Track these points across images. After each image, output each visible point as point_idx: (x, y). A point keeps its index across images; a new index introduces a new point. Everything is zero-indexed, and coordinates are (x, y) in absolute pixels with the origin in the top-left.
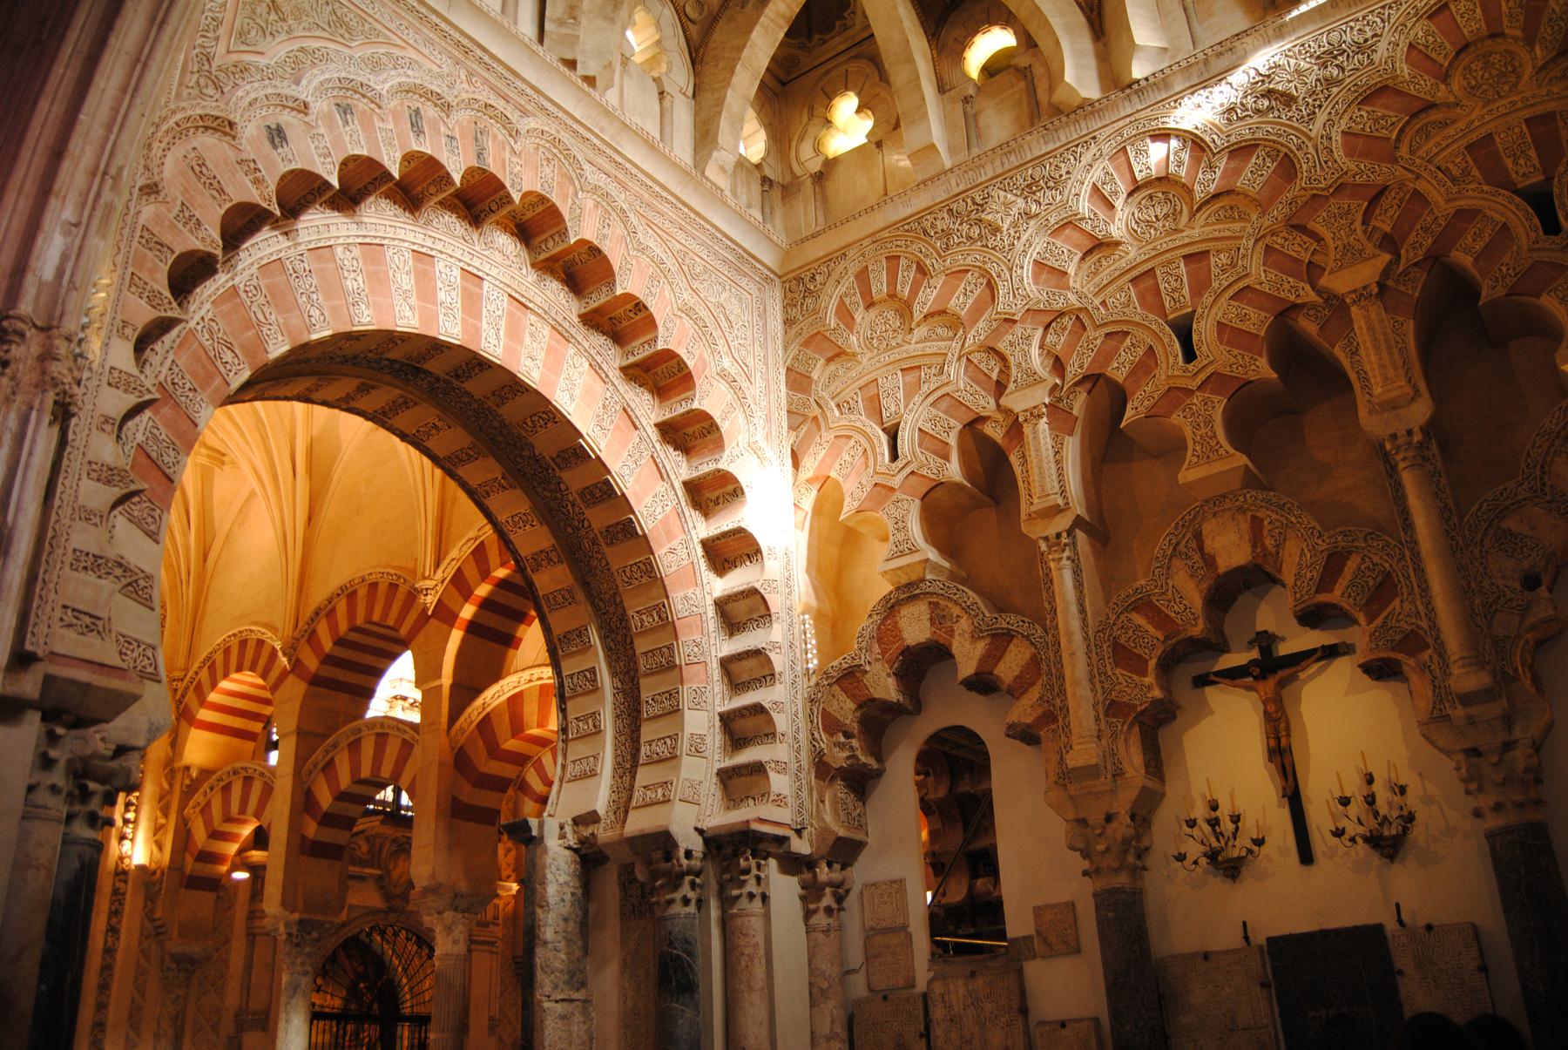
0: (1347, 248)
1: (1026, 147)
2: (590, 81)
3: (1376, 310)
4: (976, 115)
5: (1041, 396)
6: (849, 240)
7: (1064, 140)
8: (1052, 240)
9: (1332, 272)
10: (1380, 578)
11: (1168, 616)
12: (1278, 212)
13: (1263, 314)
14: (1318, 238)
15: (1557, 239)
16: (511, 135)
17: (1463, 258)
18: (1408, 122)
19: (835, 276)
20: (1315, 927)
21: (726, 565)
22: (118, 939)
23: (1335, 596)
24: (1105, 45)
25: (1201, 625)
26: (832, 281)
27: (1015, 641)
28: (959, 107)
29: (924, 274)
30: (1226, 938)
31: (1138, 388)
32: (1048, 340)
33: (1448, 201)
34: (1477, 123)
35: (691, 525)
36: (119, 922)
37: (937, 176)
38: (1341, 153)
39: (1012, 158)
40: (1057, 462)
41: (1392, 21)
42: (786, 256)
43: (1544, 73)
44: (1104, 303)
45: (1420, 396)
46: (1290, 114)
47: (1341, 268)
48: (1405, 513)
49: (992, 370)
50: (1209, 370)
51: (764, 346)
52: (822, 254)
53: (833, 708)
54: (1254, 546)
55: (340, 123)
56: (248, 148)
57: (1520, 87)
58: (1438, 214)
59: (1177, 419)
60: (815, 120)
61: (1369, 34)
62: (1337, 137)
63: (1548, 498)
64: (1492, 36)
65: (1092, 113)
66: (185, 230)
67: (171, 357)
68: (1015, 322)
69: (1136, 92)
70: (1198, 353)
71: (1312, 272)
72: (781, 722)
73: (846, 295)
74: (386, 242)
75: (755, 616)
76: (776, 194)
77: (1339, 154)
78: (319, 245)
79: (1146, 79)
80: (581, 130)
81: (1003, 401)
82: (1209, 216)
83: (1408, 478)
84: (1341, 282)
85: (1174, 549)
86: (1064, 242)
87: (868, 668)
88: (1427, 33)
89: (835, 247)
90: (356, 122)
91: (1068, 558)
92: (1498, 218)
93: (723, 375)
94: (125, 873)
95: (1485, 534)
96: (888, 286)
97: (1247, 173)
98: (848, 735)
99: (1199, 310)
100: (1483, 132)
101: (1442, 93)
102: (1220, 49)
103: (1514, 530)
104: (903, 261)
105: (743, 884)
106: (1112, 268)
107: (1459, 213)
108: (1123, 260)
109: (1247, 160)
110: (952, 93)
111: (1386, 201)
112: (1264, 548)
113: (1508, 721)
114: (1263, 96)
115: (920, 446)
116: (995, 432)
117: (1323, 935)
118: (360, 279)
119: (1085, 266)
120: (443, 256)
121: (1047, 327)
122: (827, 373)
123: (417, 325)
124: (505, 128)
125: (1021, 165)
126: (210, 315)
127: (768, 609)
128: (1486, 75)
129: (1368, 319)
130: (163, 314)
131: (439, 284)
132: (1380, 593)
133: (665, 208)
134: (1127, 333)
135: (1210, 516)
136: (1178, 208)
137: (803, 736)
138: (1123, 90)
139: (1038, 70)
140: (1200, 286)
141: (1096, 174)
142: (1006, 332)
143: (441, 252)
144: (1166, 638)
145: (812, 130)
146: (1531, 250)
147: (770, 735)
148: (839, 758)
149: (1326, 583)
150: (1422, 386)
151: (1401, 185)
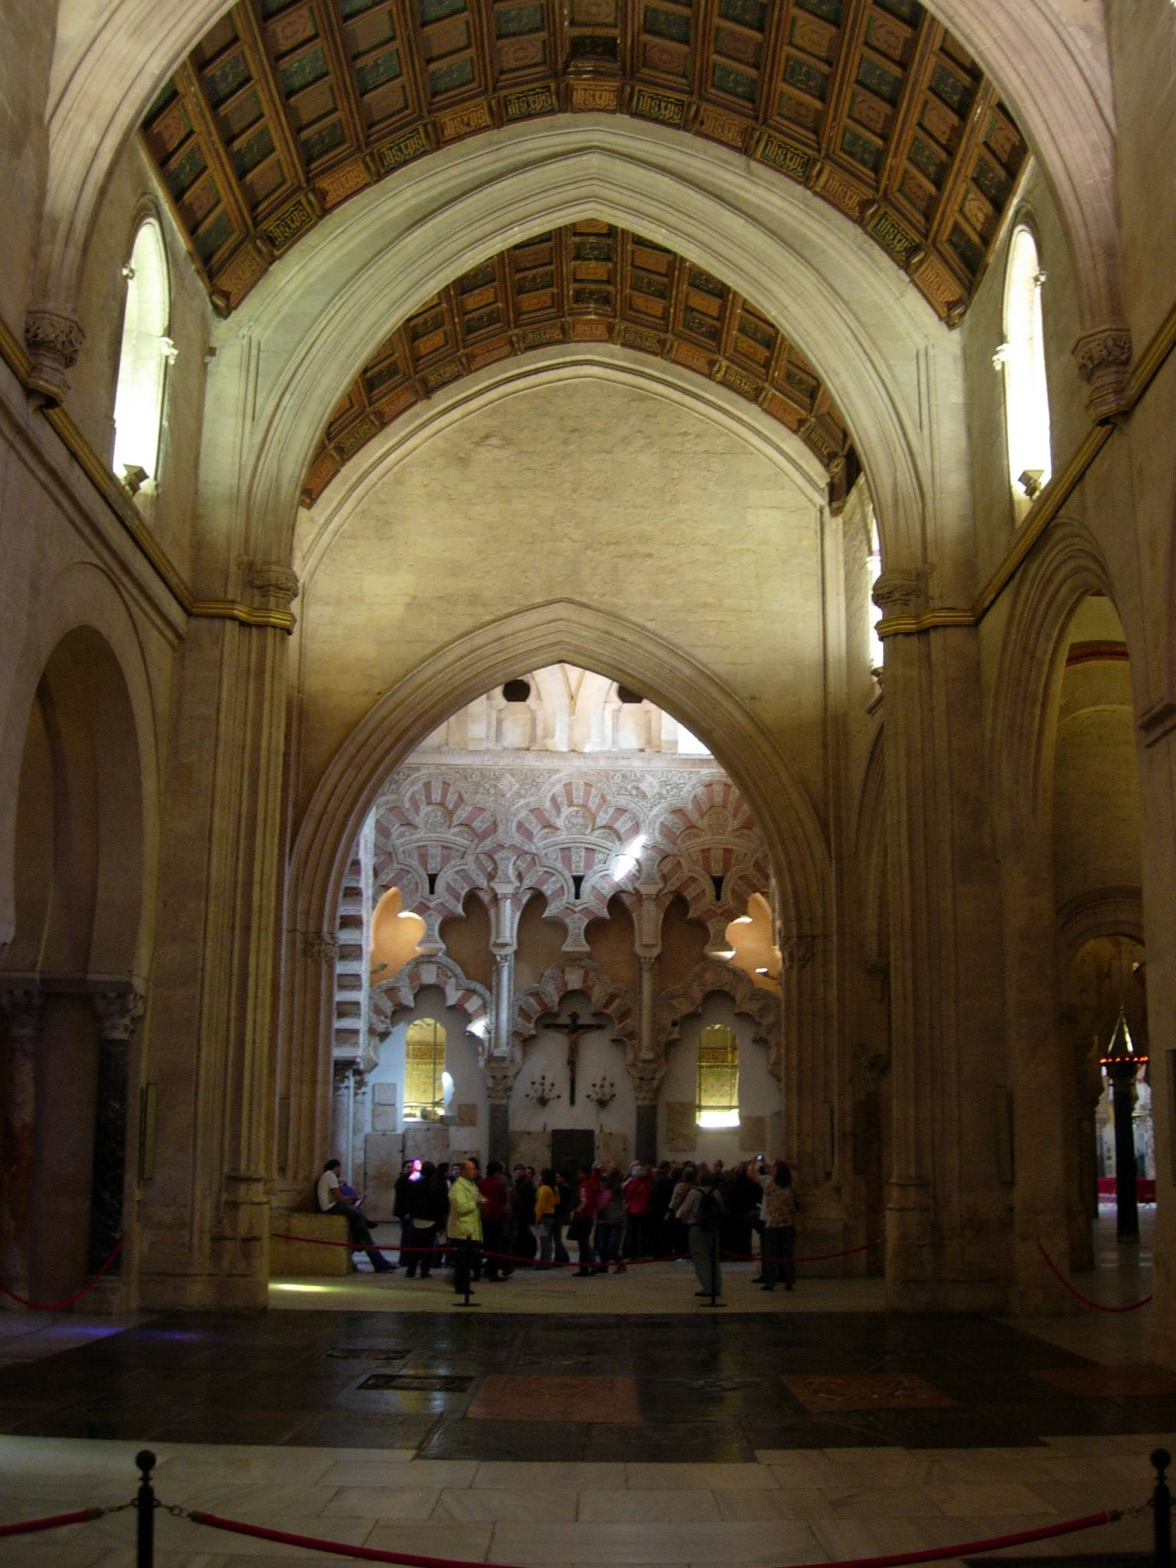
15: (719, 904)
20: (568, 1127)
23: (609, 1011)
30: (536, 1126)
53: (380, 1003)
59: (567, 920)
62: (658, 823)
81: (492, 884)
83: (646, 976)
98: (386, 1017)
104: (451, 789)
105: (342, 1082)
107: (691, 877)
109: (622, 815)
113: (655, 1071)
116: (486, 898)
117: (572, 1132)
132: (625, 1014)
134: (553, 875)
139: (540, 716)
142: (497, 851)
147: (358, 1015)
148: (381, 1028)
149: (607, 1005)
151: (675, 856)
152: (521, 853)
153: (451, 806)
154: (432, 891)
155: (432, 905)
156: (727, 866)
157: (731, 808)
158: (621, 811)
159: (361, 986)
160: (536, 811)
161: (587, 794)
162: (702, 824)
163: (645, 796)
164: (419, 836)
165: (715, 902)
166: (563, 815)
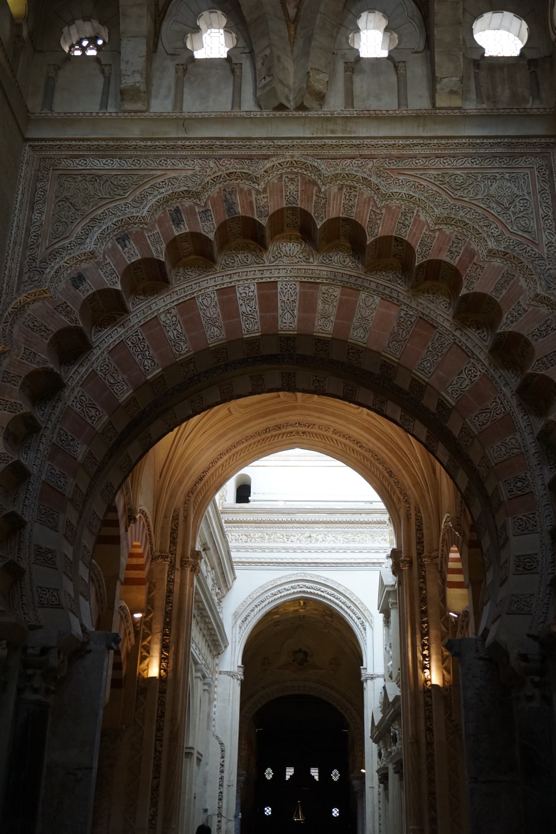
2: (301, 107)
16: (254, 182)
22: (433, 735)
36: (431, 725)
55: (120, 249)
56: (61, 297)
66: (26, 362)
67: (59, 426)
74: (195, 295)
78: (147, 320)
80: (316, 142)
90: (132, 242)
93: (492, 253)
94: (429, 691)
118: (178, 327)
120: (241, 282)
123: (225, 337)
124: (248, 180)
126: (80, 394)
130: (18, 413)
131: (240, 302)
133: (417, 151)
143: (239, 281)
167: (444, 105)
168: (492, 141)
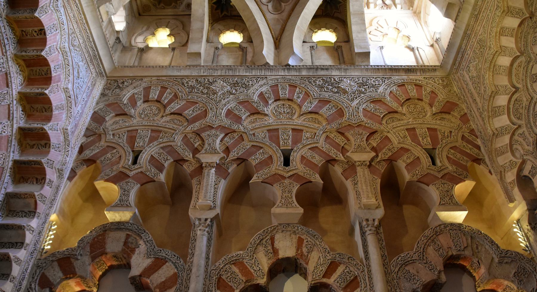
0: (359, 146)
1: (238, 70)
3: (367, 171)
4: (218, 56)
5: (216, 159)
6: (146, 74)
7: (254, 74)
8: (238, 105)
9: (352, 152)
10: (352, 278)
11: (250, 271)
12: (335, 125)
13: (321, 158)
14: (348, 140)
17: (401, 164)
18: (386, 114)
19: (134, 85)
21: (22, 180)
23: (331, 281)
24: (278, 52)
25: (265, 280)
26: (132, 86)
27: (167, 264)
28: (213, 49)
29: (177, 98)
31: (261, 169)
32: (225, 139)
33: (399, 143)
34: (410, 123)
35: (12, 150)
37: (197, 66)
38: (362, 114)
39: (231, 72)
40: (215, 188)
41: (386, 82)
42: (115, 69)
43: (434, 116)
44: (254, 134)
45: (380, 207)
46: (344, 96)
47: (356, 152)
48: (366, 252)
49: (196, 143)
50: (295, 172)
51: (88, 96)
52: (131, 75)
54: (297, 250)
57: (426, 118)
58: (394, 146)
60: (148, 31)
61: (377, 83)
63: (425, 261)
64: (419, 99)
65: (268, 69)
68: (213, 128)
69: (288, 69)
70: (291, 164)
71: (343, 150)
72: (16, 270)
73: (136, 94)
75: (26, 210)
76: (120, 48)
77: (361, 114)
79: (293, 66)
81: (197, 156)
82: (306, 119)
84: (357, 157)
85: (260, 241)
86: (243, 107)
87: (79, 257)
88: (397, 90)
89: (139, 75)
91: (208, 232)
92: (417, 155)
95: (399, 270)
96: (158, 97)
97: (325, 109)
99: (295, 149)
100: (412, 126)
101: (400, 109)
102: (323, 67)
103: (410, 271)
104: (168, 90)
106: (261, 123)
107: (402, 148)
108: (266, 122)
110: (212, 44)
111: (375, 136)
112: (302, 252)
114: (335, 88)
115: (149, 162)
116: (188, 168)
119: (249, 119)
121: (226, 135)
122: (113, 120)
125: (233, 76)
127: (36, 208)
128: (415, 110)
129: (364, 172)
134: (262, 148)
135: (280, 231)
136: (294, 112)
137: (25, 283)
138: (283, 66)
139: (250, 50)
140: (296, 141)
141: (264, 89)
142: (208, 130)
144: (247, 281)
145: (145, 34)
146: (428, 169)
149: (328, 273)
150: (381, 204)
151: (382, 132)
152: (228, 132)
153: (166, 101)
154: (135, 162)
155: (131, 174)
156: (435, 140)
157: (426, 100)
158: (324, 102)
159: (23, 243)
160: (246, 103)
161: (292, 92)
162: (404, 110)
163: (345, 92)
164: (131, 123)
165: (433, 167)
166: (271, 107)
167: (101, 11)
168: (94, 46)
